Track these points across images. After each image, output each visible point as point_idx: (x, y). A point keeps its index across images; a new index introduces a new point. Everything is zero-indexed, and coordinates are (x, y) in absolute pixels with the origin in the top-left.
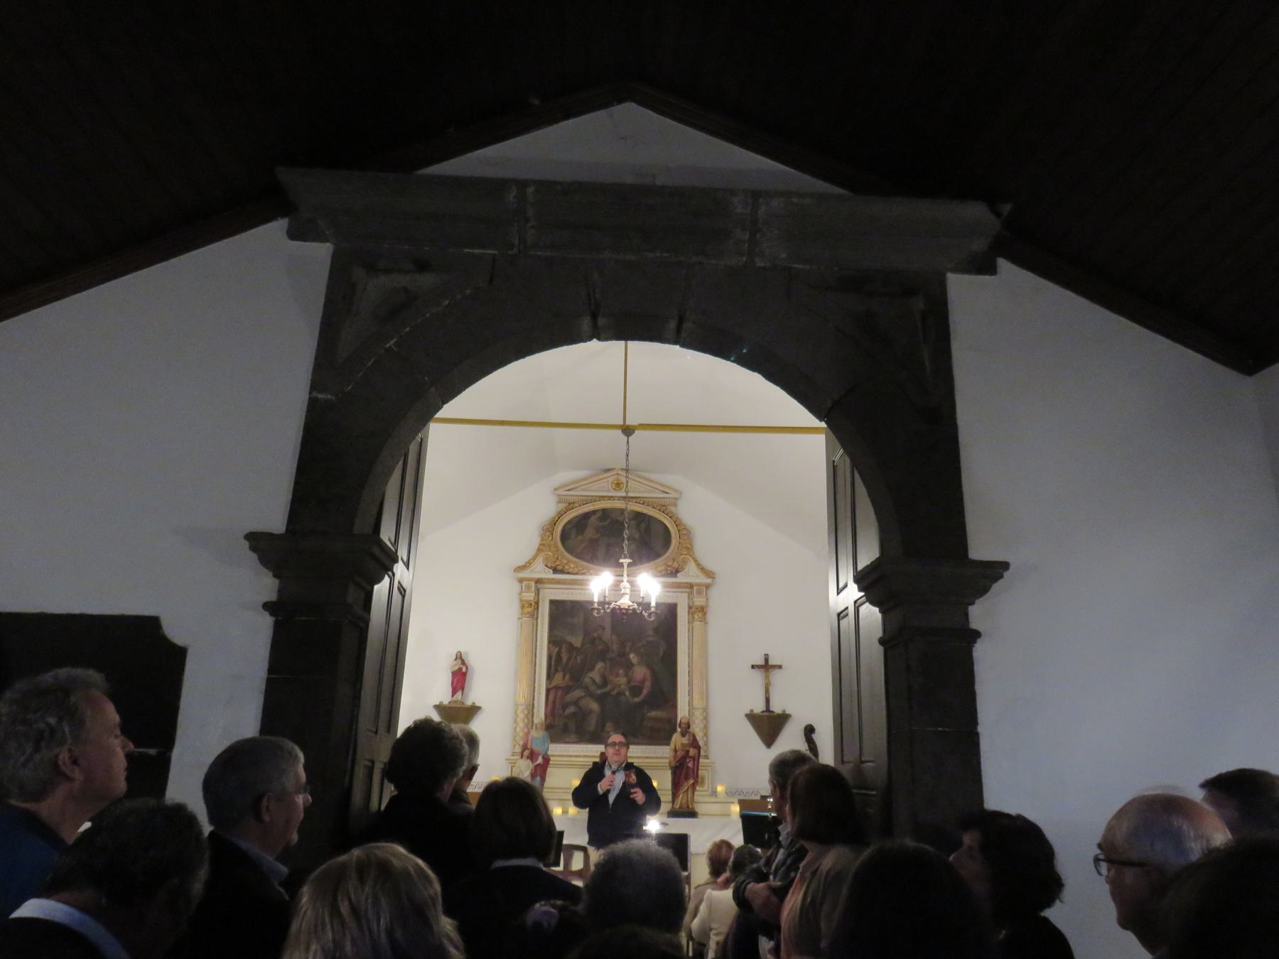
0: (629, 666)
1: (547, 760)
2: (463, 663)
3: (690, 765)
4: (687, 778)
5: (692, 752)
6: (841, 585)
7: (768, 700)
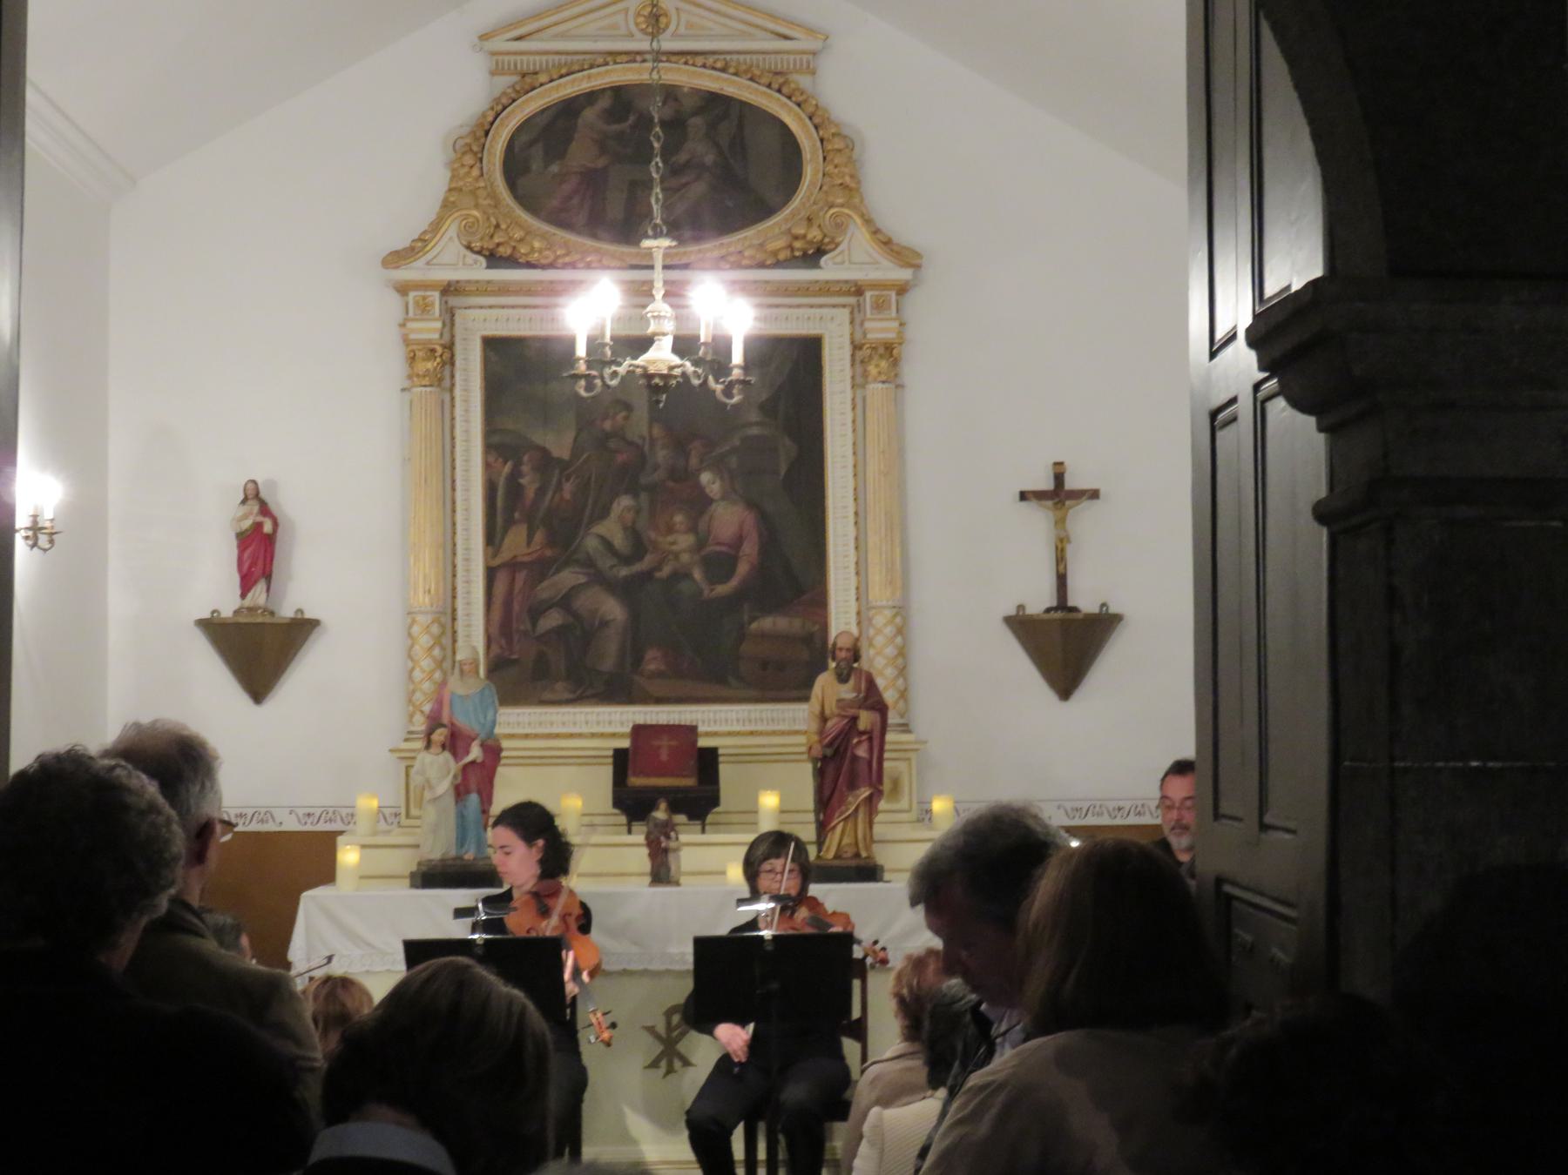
0: (700, 503)
1: (493, 753)
2: (265, 510)
3: (862, 752)
4: (853, 786)
5: (866, 719)
6: (1220, 334)
7: (1062, 581)
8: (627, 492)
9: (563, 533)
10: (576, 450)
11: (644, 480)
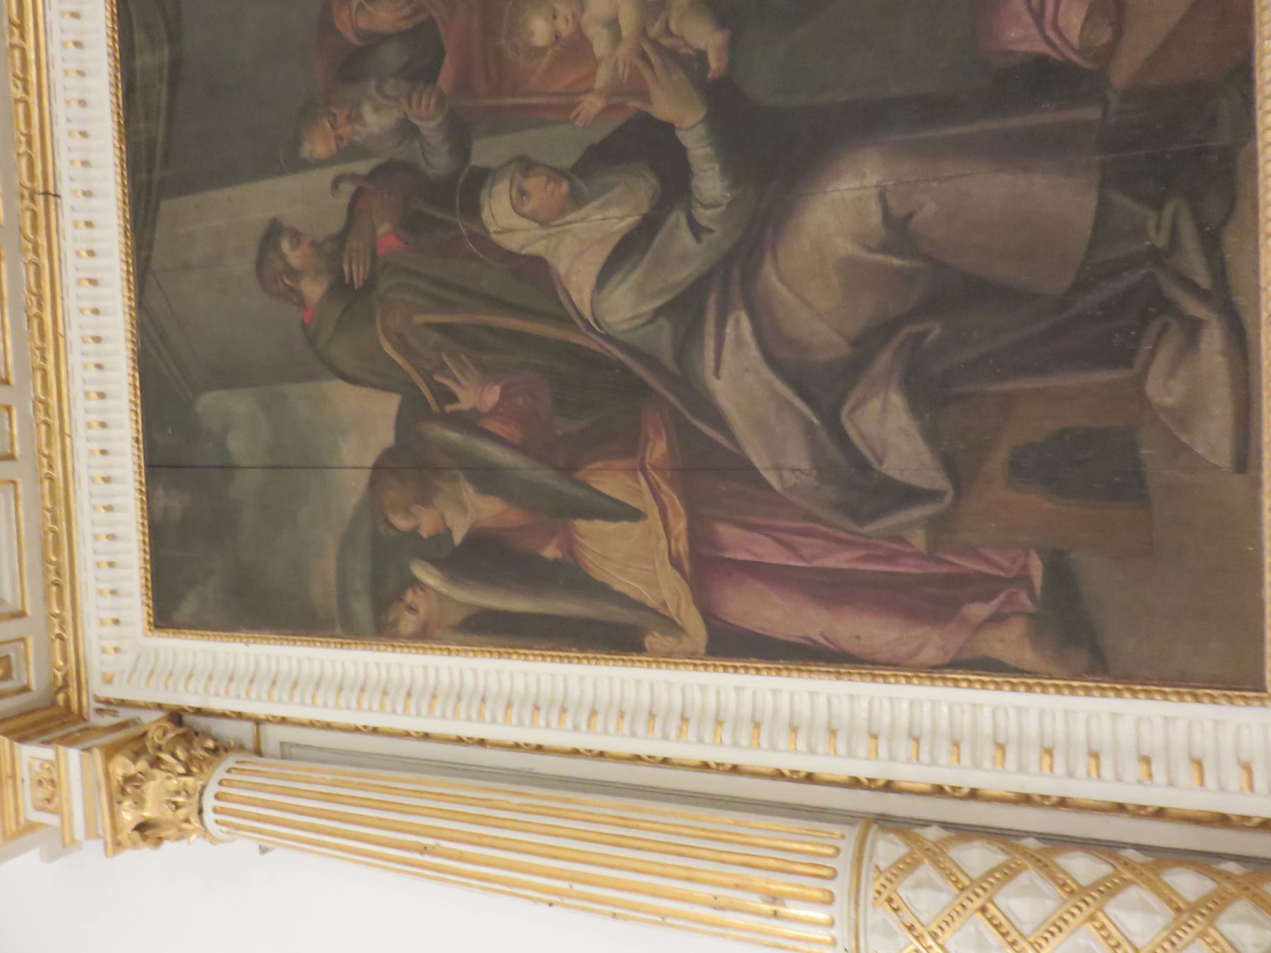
8: (473, 210)
9: (605, 400)
10: (376, 377)
11: (440, 163)
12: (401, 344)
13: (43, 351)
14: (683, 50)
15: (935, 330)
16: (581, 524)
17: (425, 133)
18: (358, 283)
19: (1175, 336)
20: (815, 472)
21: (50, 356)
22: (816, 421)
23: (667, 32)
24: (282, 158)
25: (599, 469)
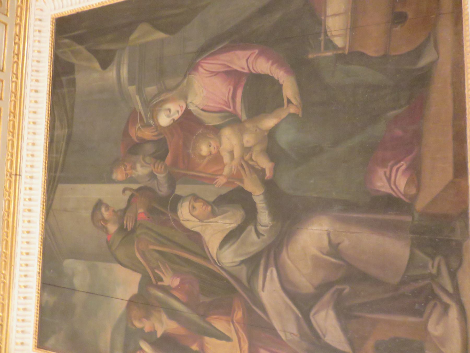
0: (189, 123)
8: (175, 210)
11: (163, 190)
12: (143, 255)
13: (7, 233)
14: (257, 167)
15: (347, 289)
16: (207, 339)
17: (159, 178)
18: (129, 229)
19: (439, 309)
20: (299, 335)
21: (10, 235)
22: (300, 316)
23: (251, 159)
24: (105, 178)
25: (216, 318)
